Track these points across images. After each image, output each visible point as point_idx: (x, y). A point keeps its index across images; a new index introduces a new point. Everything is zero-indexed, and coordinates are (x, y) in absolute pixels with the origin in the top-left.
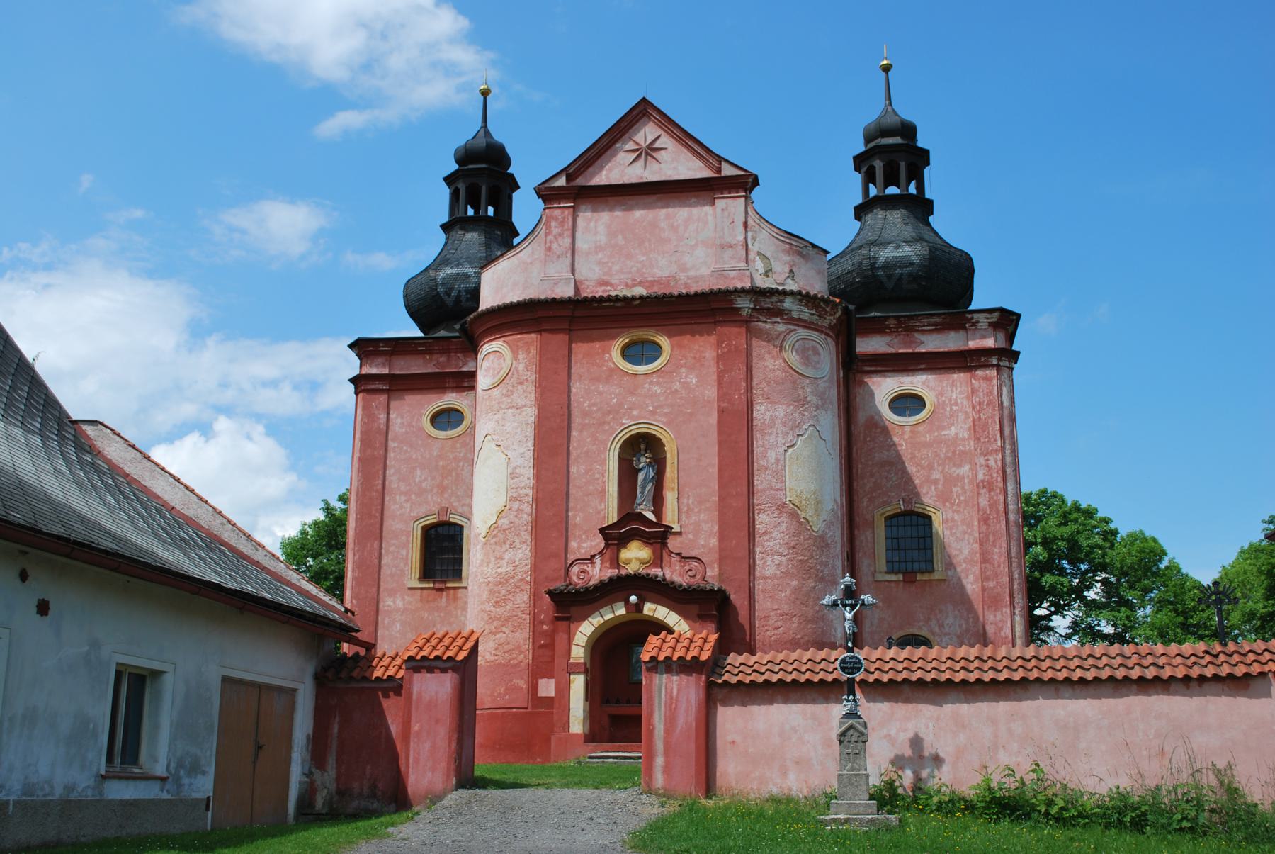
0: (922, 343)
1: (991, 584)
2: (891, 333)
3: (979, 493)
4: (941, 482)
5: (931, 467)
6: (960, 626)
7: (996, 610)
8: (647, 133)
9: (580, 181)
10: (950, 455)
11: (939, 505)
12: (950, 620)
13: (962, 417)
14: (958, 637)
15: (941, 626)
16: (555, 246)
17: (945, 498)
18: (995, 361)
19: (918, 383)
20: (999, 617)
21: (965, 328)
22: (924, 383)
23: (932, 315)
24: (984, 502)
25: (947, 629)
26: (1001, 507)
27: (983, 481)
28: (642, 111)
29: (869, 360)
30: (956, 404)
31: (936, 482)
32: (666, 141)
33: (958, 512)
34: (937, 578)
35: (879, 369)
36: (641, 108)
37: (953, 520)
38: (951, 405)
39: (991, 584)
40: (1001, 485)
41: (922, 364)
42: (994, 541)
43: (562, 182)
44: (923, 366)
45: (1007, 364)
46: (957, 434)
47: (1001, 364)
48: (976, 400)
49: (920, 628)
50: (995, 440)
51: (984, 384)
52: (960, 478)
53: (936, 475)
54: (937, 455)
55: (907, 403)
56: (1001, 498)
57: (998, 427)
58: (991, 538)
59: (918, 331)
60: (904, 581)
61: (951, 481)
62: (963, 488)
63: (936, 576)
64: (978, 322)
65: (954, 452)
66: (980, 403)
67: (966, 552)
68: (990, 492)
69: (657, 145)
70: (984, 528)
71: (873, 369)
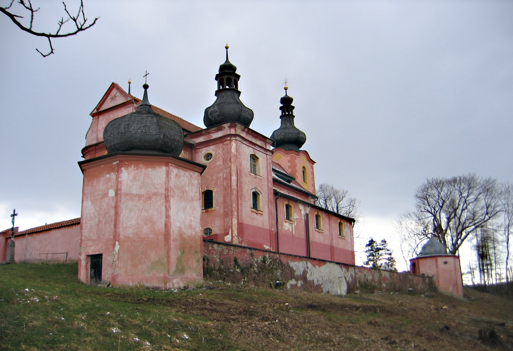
0: (212, 137)
1: (226, 209)
2: (205, 135)
3: (224, 181)
4: (215, 180)
5: (213, 176)
6: (219, 224)
7: (227, 217)
8: (114, 92)
9: (100, 110)
10: (218, 170)
11: (215, 187)
12: (216, 222)
13: (221, 158)
14: (218, 227)
15: (214, 224)
16: (94, 130)
17: (216, 184)
18: (229, 139)
19: (211, 149)
20: (228, 219)
21: (222, 130)
22: (212, 149)
23: (213, 127)
24: (225, 184)
25: (216, 225)
26: (229, 185)
27: (225, 177)
28: (113, 86)
29: (198, 145)
30: (220, 154)
31: (214, 180)
32: (118, 94)
33: (219, 188)
34: (214, 209)
35: (201, 147)
36: (113, 85)
37: (218, 191)
38: (219, 155)
39: (226, 209)
40: (229, 178)
41: (211, 143)
42: (227, 196)
43: (95, 111)
44: (212, 144)
45: (234, 139)
46: (220, 164)
47: (232, 139)
48: (224, 152)
49: (209, 226)
50: (228, 164)
51: (226, 146)
52: (220, 177)
53: (214, 178)
54: (215, 171)
55: (208, 156)
56: (229, 182)
57: (229, 160)
58: (227, 195)
59: (211, 133)
60: (206, 212)
61: (218, 179)
62: (221, 180)
63: (213, 209)
64: (225, 127)
65: (219, 170)
66: (225, 153)
67: (221, 200)
68: (227, 180)
69: (116, 95)
70: (225, 192)
71: (200, 147)
